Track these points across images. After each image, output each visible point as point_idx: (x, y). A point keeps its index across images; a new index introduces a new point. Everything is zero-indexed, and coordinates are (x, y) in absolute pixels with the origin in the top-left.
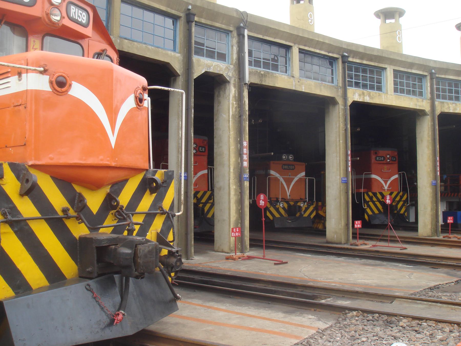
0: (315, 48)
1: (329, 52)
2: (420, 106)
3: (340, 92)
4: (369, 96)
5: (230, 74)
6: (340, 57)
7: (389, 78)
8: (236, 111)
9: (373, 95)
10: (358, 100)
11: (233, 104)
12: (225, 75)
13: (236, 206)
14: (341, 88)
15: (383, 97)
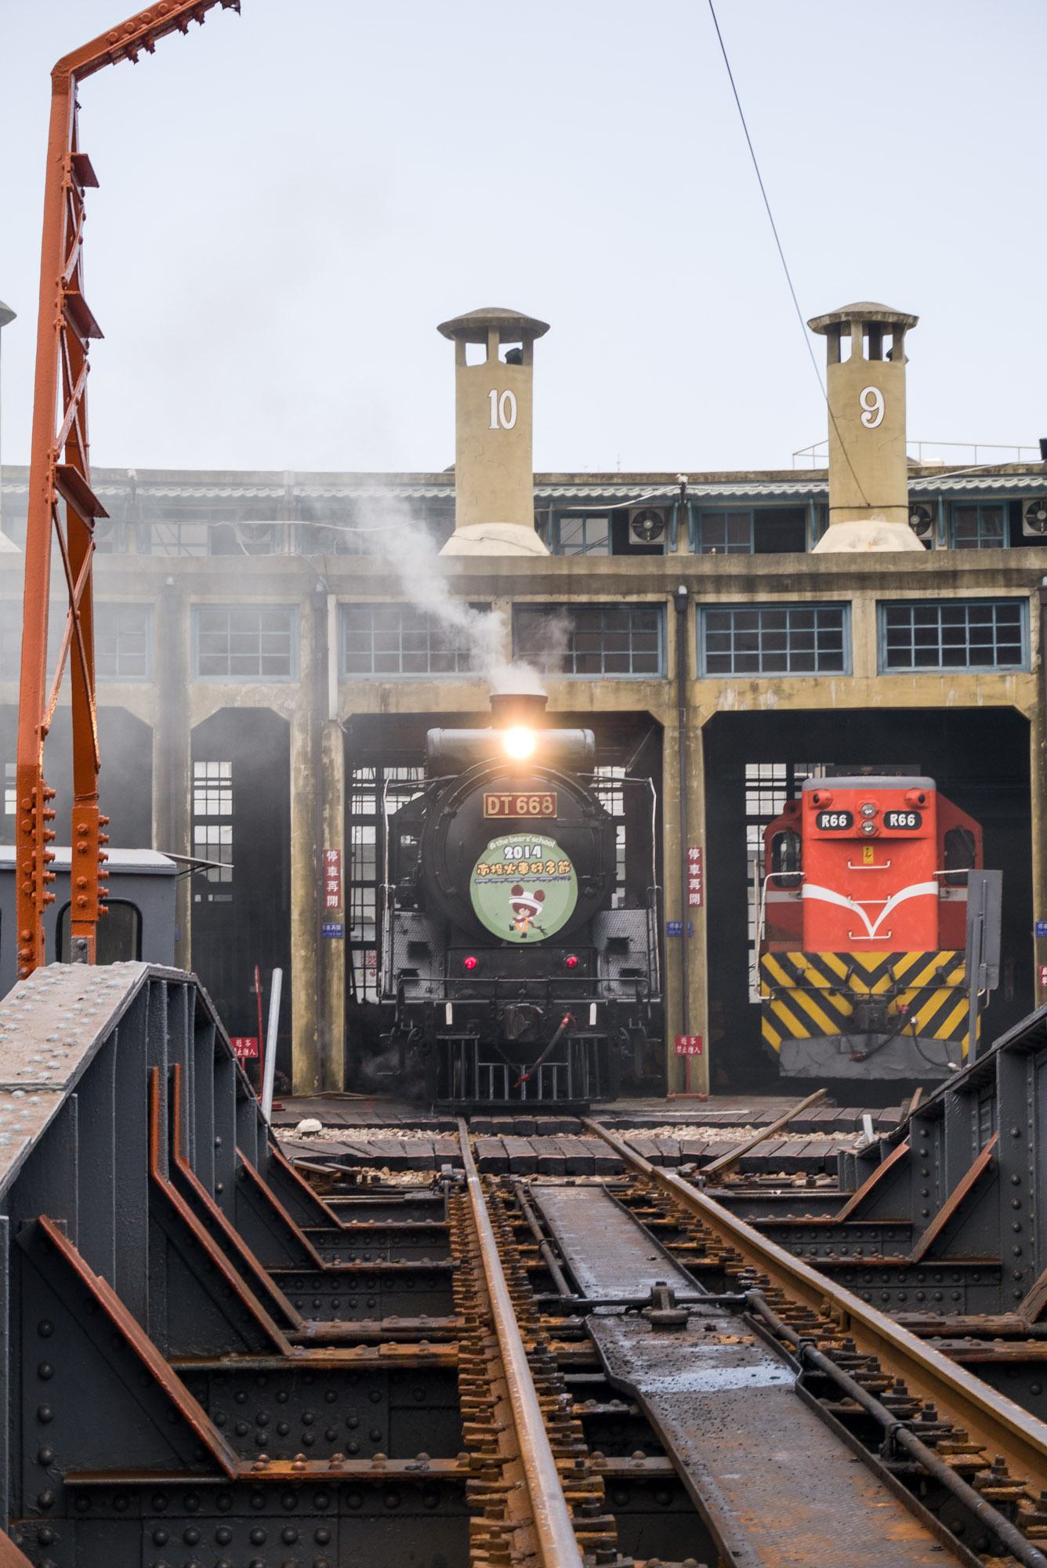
0: (570, 592)
1: (625, 594)
2: (990, 697)
3: (669, 693)
4: (778, 691)
5: (293, 705)
6: (670, 598)
7: (863, 629)
8: (305, 785)
9: (792, 688)
10: (736, 708)
11: (298, 770)
12: (275, 708)
13: (308, 995)
14: (670, 683)
15: (833, 687)
